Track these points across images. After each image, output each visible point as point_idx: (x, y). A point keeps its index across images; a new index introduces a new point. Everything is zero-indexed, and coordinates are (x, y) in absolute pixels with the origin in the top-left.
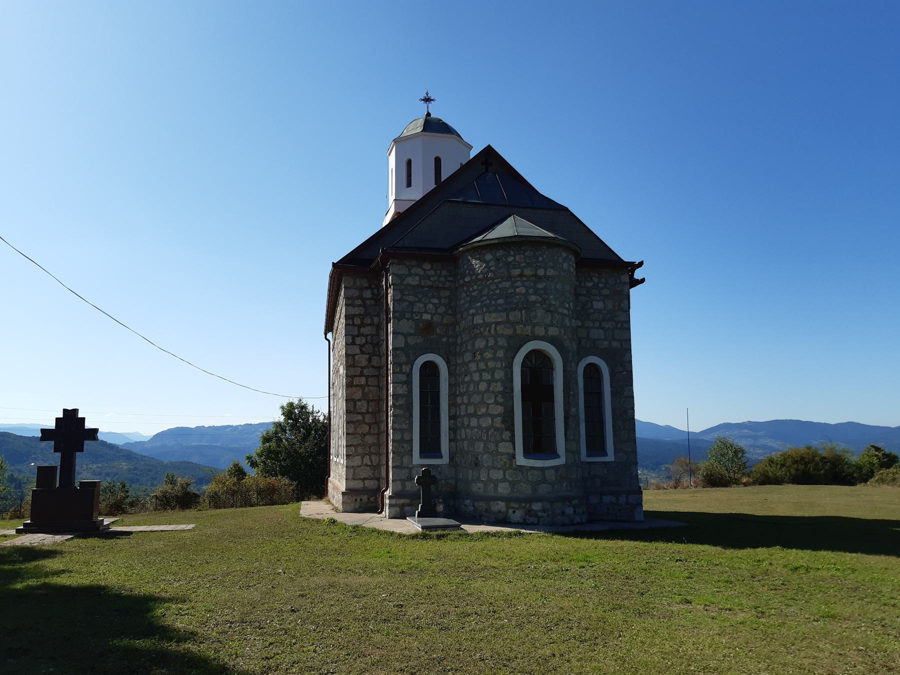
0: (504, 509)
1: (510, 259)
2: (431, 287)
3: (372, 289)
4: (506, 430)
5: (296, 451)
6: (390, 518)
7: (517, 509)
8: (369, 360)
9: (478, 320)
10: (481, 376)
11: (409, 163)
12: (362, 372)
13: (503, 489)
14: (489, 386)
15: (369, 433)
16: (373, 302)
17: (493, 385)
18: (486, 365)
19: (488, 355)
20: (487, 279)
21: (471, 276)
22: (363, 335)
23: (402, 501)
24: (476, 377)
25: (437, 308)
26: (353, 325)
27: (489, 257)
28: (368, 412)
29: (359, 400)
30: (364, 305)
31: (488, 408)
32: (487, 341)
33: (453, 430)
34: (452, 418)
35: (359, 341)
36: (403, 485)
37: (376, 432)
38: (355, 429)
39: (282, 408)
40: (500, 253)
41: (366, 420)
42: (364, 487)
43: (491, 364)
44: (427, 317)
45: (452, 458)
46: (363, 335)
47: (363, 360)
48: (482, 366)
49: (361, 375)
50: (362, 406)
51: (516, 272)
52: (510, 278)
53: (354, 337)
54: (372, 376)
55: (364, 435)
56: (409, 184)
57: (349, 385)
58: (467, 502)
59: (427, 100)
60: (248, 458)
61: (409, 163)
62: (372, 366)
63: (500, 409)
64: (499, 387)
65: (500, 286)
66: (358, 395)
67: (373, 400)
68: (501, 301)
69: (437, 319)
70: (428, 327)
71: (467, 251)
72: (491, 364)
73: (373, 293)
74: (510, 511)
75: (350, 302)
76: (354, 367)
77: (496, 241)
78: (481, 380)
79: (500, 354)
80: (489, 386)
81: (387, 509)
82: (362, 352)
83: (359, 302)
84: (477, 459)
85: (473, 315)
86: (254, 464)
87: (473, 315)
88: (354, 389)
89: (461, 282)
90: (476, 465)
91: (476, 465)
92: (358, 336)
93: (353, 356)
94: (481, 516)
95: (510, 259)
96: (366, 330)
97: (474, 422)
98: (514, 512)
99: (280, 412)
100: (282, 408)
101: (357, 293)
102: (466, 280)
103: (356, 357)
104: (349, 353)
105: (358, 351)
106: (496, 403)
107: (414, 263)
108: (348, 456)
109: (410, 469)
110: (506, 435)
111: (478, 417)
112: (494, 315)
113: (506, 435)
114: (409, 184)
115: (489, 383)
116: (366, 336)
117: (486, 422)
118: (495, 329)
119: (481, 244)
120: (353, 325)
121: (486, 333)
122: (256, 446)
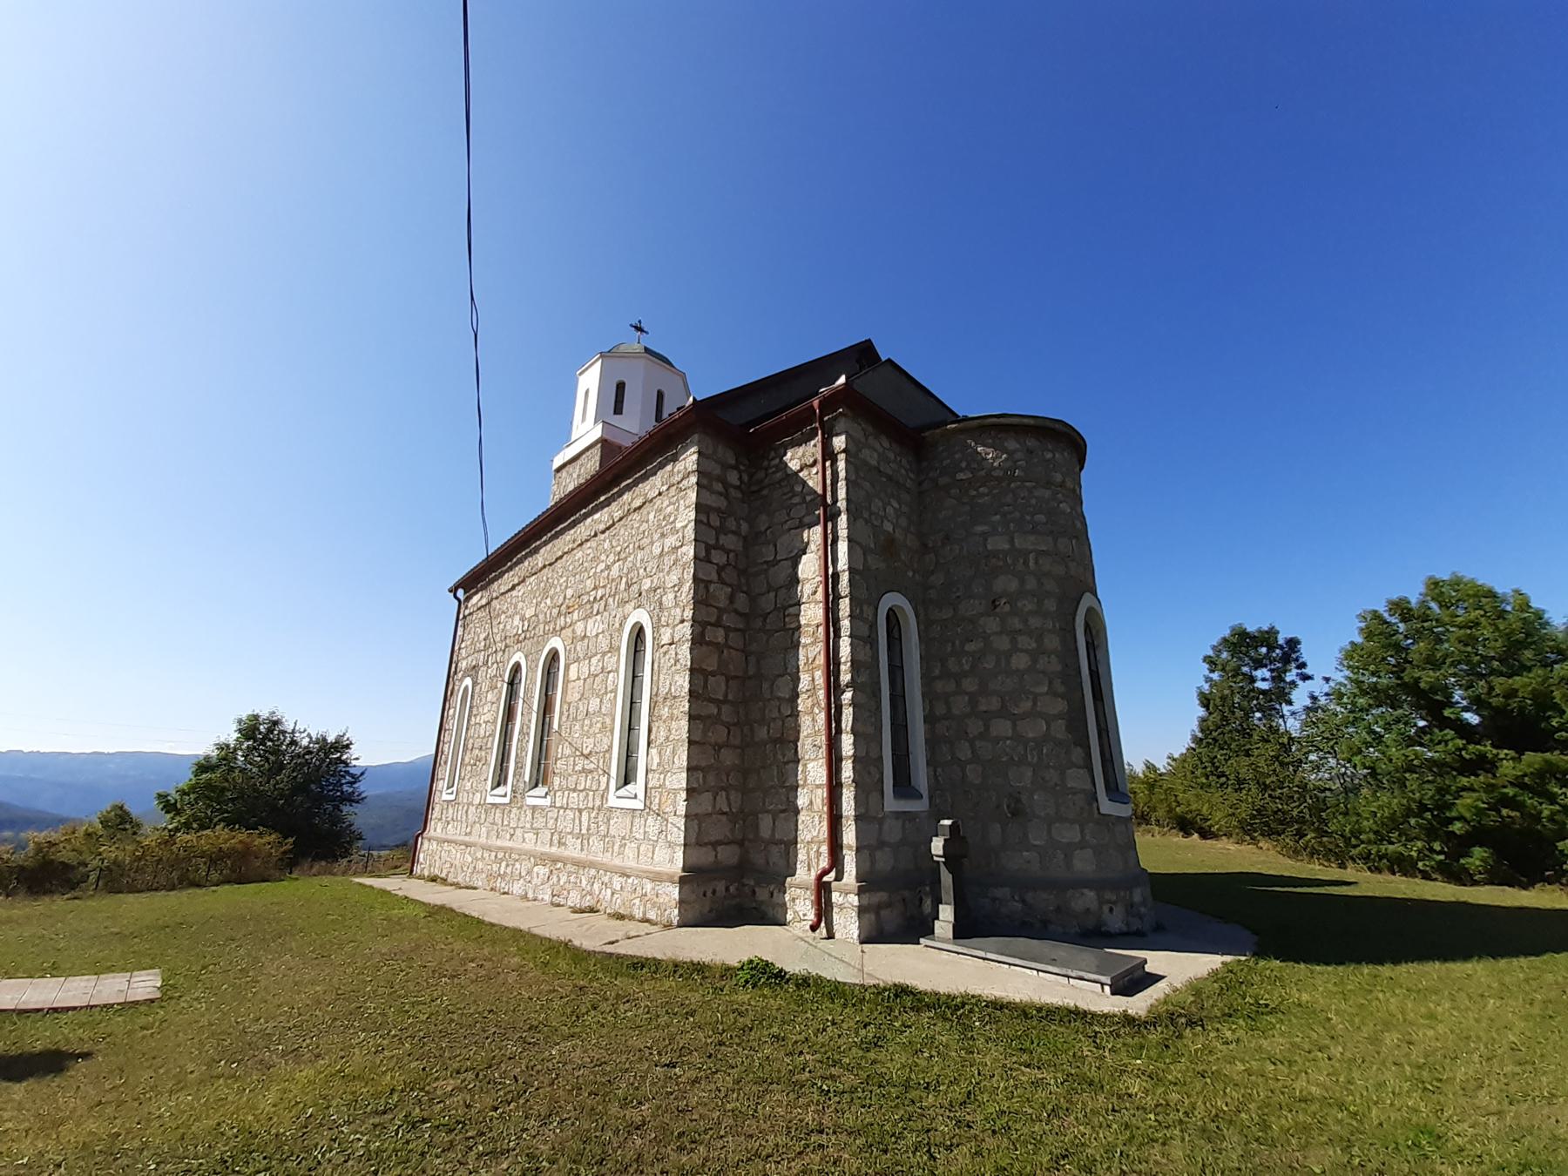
0: (1094, 906)
1: (1049, 456)
2: (890, 478)
3: (740, 472)
4: (1076, 744)
5: (256, 790)
6: (865, 940)
7: (1115, 903)
8: (731, 598)
9: (998, 543)
10: (1014, 641)
11: (621, 387)
12: (719, 618)
13: (1084, 863)
14: (1035, 661)
15: (727, 745)
16: (739, 495)
17: (1042, 663)
18: (1026, 622)
19: (1027, 605)
20: (1013, 478)
21: (973, 471)
22: (722, 548)
23: (881, 896)
24: (1003, 643)
25: (898, 517)
26: (708, 524)
27: (1012, 444)
28: (725, 701)
29: (713, 674)
30: (726, 496)
31: (1035, 704)
32: (1022, 582)
33: (932, 743)
34: (929, 719)
35: (718, 557)
36: (873, 862)
37: (737, 742)
38: (705, 732)
39: (240, 721)
40: (1031, 443)
41: (723, 717)
42: (716, 862)
43: (1035, 622)
44: (888, 527)
45: (931, 798)
46: (722, 548)
47: (721, 594)
48: (1016, 623)
49: (717, 624)
50: (718, 686)
51: (1058, 477)
52: (1048, 484)
53: (708, 548)
54: (737, 630)
55: (718, 747)
56: (618, 410)
57: (697, 641)
58: (1000, 892)
59: (639, 329)
60: (160, 796)
61: (621, 387)
62: (736, 612)
63: (1061, 706)
64: (1055, 666)
65: (1036, 493)
66: (711, 664)
67: (736, 677)
68: (1041, 518)
69: (898, 535)
70: (888, 547)
71: (961, 431)
72: (1035, 622)
73: (740, 478)
74: (1106, 908)
75: (705, 482)
76: (708, 605)
77: (1032, 422)
78: (1015, 648)
79: (1051, 605)
80: (1035, 661)
81: (847, 923)
82: (722, 581)
83: (719, 487)
84: (1018, 801)
85: (985, 536)
86: (169, 807)
87: (985, 536)
88: (704, 648)
89: (943, 481)
90: (1016, 813)
91: (1016, 813)
92: (716, 547)
93: (707, 583)
94: (1045, 923)
95: (1049, 456)
96: (729, 541)
97: (1002, 727)
98: (1111, 910)
99: (235, 727)
100: (240, 721)
101: (717, 471)
102: (961, 476)
103: (712, 588)
104: (700, 576)
105: (714, 577)
106: (1056, 695)
107: (870, 429)
108: (690, 791)
109: (881, 822)
110: (1077, 754)
111: (1014, 719)
112: (1032, 538)
113: (1077, 754)
114: (618, 410)
115: (1034, 656)
116: (728, 552)
117: (1034, 730)
118: (1036, 563)
119: (1002, 420)
120: (708, 524)
121: (1020, 567)
122: (186, 778)
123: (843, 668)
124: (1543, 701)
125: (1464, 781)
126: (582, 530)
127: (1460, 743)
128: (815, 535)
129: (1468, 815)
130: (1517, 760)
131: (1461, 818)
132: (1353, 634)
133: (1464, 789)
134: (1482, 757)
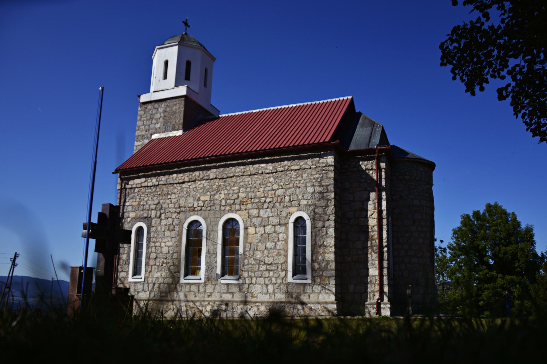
123: (384, 241)
124: (514, 256)
125: (486, 286)
126: (251, 169)
127: (487, 271)
128: (373, 195)
129: (485, 299)
130: (503, 278)
131: (483, 300)
132: (457, 223)
133: (485, 289)
134: (492, 276)
